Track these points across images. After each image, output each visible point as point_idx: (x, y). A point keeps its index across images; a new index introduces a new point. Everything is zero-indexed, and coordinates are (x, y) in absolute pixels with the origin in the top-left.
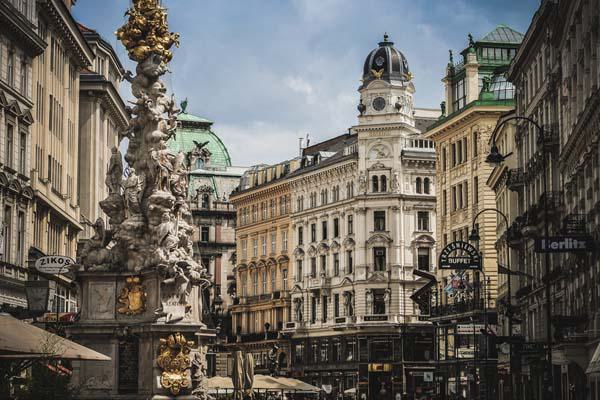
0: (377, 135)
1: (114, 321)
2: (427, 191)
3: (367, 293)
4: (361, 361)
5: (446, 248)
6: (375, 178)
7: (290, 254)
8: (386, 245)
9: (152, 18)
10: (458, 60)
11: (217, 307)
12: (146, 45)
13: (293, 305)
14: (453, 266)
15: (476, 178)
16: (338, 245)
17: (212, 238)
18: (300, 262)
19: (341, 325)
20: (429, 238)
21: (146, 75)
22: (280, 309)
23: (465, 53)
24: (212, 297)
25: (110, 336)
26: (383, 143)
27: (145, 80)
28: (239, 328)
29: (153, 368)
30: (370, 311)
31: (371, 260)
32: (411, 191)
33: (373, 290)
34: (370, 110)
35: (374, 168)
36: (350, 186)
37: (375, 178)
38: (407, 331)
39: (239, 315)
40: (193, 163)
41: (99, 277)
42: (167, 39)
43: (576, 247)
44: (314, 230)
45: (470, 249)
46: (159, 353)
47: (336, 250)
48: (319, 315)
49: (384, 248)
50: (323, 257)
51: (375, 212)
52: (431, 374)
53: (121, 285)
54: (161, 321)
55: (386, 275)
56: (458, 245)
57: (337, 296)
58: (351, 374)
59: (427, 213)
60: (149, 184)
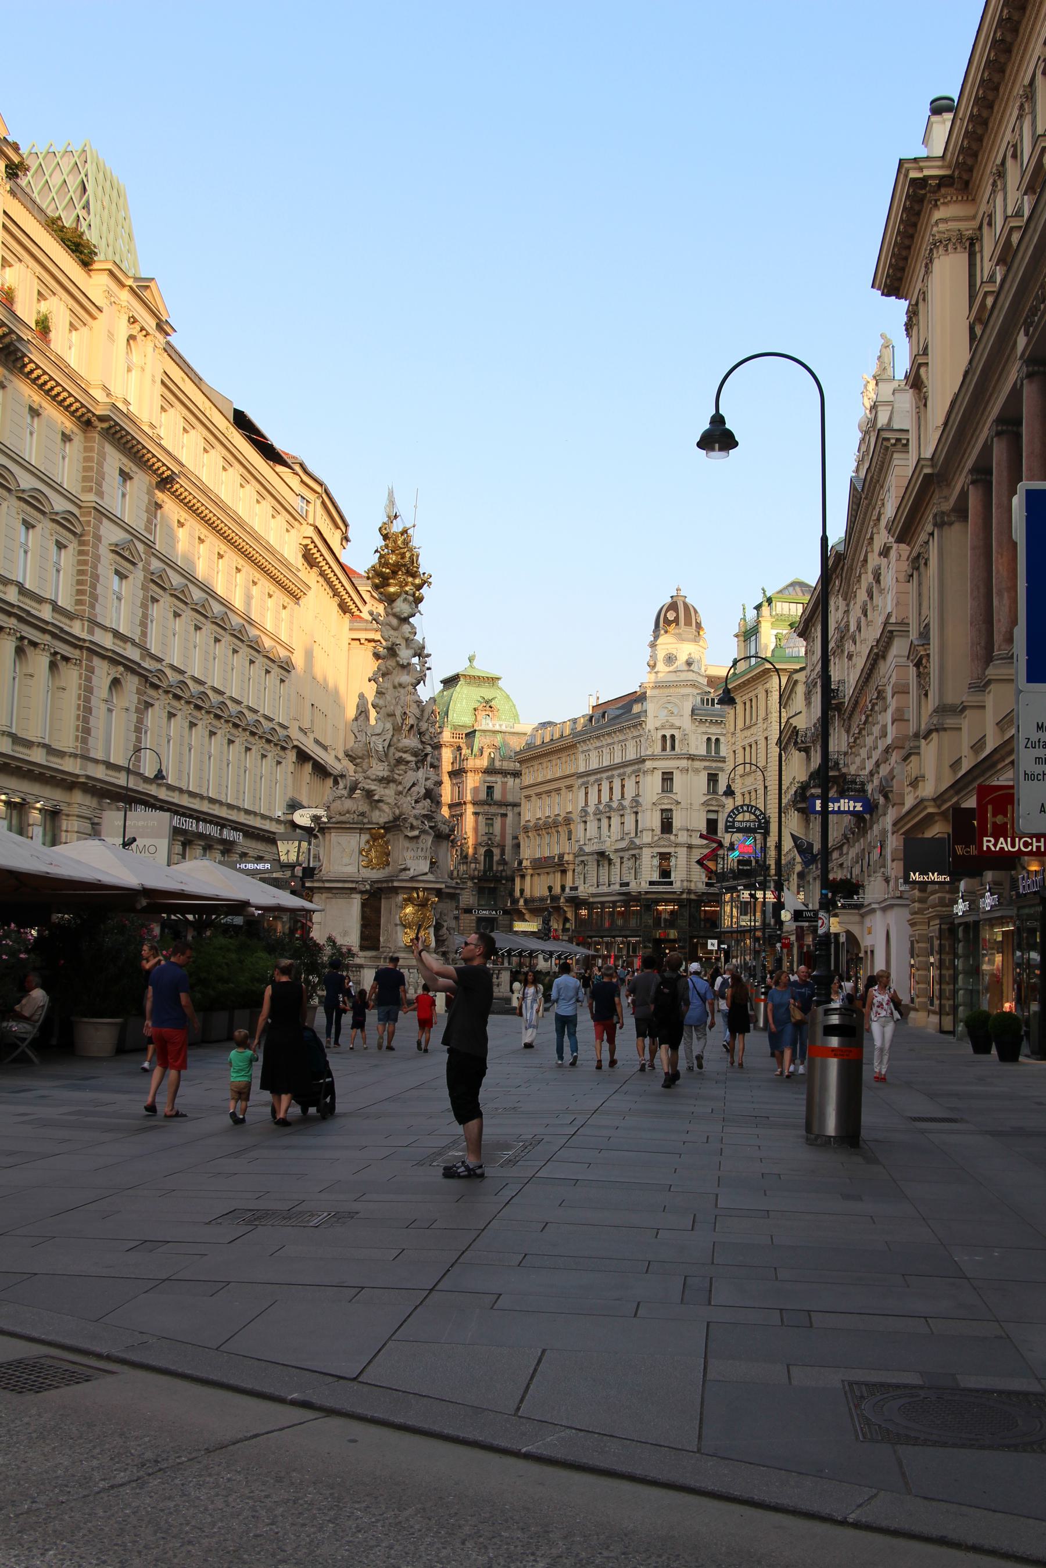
0: (667, 691)
1: (356, 875)
2: (717, 751)
3: (653, 857)
5: (732, 811)
6: (664, 736)
7: (575, 816)
8: (673, 807)
9: (403, 556)
10: (751, 614)
11: (501, 868)
12: (396, 585)
13: (579, 869)
14: (740, 830)
15: (766, 738)
16: (624, 808)
17: (497, 795)
18: (585, 822)
19: (624, 889)
20: (717, 800)
21: (395, 615)
22: (564, 872)
23: (758, 608)
24: (496, 858)
25: (353, 890)
27: (395, 622)
28: (522, 891)
29: (396, 925)
30: (656, 877)
31: (657, 824)
32: (702, 751)
33: (661, 854)
34: (661, 666)
35: (663, 727)
36: (638, 745)
37: (664, 736)
38: (693, 897)
39: (523, 877)
40: (479, 718)
41: (343, 827)
42: (417, 581)
43: (851, 809)
44: (600, 791)
45: (758, 813)
46: (403, 908)
47: (621, 812)
48: (604, 879)
49: (671, 810)
50: (609, 818)
52: (715, 942)
53: (365, 837)
54: (404, 876)
56: (745, 808)
57: (622, 858)
58: (633, 940)
60: (397, 729)
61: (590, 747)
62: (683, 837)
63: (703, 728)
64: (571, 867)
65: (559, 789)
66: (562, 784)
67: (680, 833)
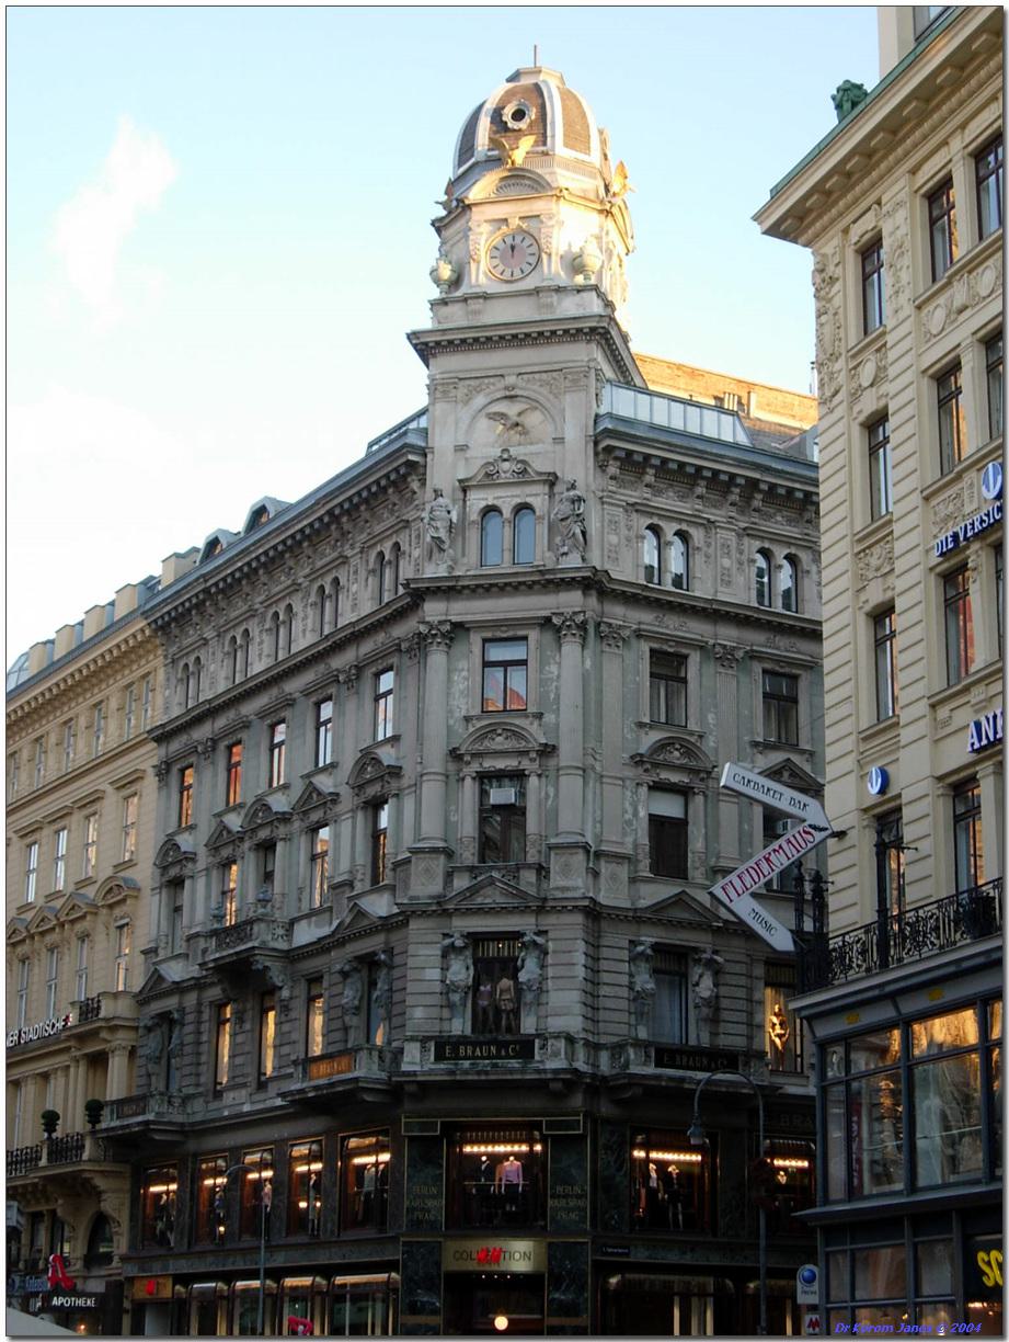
3: (448, 952)
4: (416, 1225)
8: (526, 764)
26: (524, 387)
33: (476, 939)
35: (490, 478)
51: (485, 641)
55: (529, 876)
59: (686, 657)
61: (209, 634)
62: (569, 879)
63: (634, 495)
64: (123, 1039)
65: (96, 798)
66: (100, 781)
67: (555, 864)
